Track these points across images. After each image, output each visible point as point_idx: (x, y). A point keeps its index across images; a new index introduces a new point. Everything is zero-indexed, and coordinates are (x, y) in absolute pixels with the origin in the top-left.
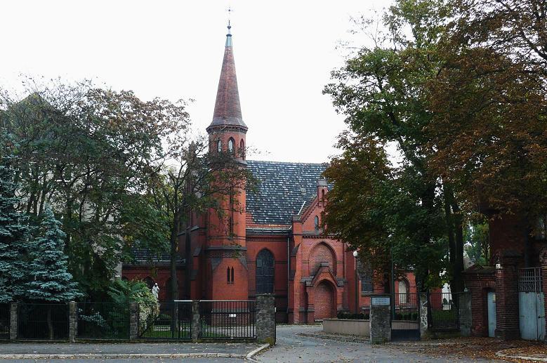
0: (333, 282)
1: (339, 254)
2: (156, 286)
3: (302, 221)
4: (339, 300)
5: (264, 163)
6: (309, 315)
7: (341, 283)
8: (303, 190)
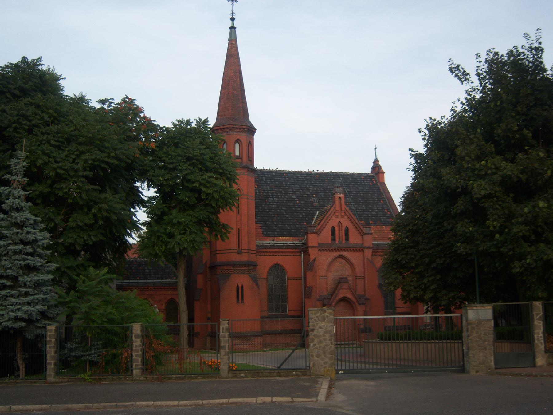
0: (354, 300)
1: (359, 269)
3: (318, 233)
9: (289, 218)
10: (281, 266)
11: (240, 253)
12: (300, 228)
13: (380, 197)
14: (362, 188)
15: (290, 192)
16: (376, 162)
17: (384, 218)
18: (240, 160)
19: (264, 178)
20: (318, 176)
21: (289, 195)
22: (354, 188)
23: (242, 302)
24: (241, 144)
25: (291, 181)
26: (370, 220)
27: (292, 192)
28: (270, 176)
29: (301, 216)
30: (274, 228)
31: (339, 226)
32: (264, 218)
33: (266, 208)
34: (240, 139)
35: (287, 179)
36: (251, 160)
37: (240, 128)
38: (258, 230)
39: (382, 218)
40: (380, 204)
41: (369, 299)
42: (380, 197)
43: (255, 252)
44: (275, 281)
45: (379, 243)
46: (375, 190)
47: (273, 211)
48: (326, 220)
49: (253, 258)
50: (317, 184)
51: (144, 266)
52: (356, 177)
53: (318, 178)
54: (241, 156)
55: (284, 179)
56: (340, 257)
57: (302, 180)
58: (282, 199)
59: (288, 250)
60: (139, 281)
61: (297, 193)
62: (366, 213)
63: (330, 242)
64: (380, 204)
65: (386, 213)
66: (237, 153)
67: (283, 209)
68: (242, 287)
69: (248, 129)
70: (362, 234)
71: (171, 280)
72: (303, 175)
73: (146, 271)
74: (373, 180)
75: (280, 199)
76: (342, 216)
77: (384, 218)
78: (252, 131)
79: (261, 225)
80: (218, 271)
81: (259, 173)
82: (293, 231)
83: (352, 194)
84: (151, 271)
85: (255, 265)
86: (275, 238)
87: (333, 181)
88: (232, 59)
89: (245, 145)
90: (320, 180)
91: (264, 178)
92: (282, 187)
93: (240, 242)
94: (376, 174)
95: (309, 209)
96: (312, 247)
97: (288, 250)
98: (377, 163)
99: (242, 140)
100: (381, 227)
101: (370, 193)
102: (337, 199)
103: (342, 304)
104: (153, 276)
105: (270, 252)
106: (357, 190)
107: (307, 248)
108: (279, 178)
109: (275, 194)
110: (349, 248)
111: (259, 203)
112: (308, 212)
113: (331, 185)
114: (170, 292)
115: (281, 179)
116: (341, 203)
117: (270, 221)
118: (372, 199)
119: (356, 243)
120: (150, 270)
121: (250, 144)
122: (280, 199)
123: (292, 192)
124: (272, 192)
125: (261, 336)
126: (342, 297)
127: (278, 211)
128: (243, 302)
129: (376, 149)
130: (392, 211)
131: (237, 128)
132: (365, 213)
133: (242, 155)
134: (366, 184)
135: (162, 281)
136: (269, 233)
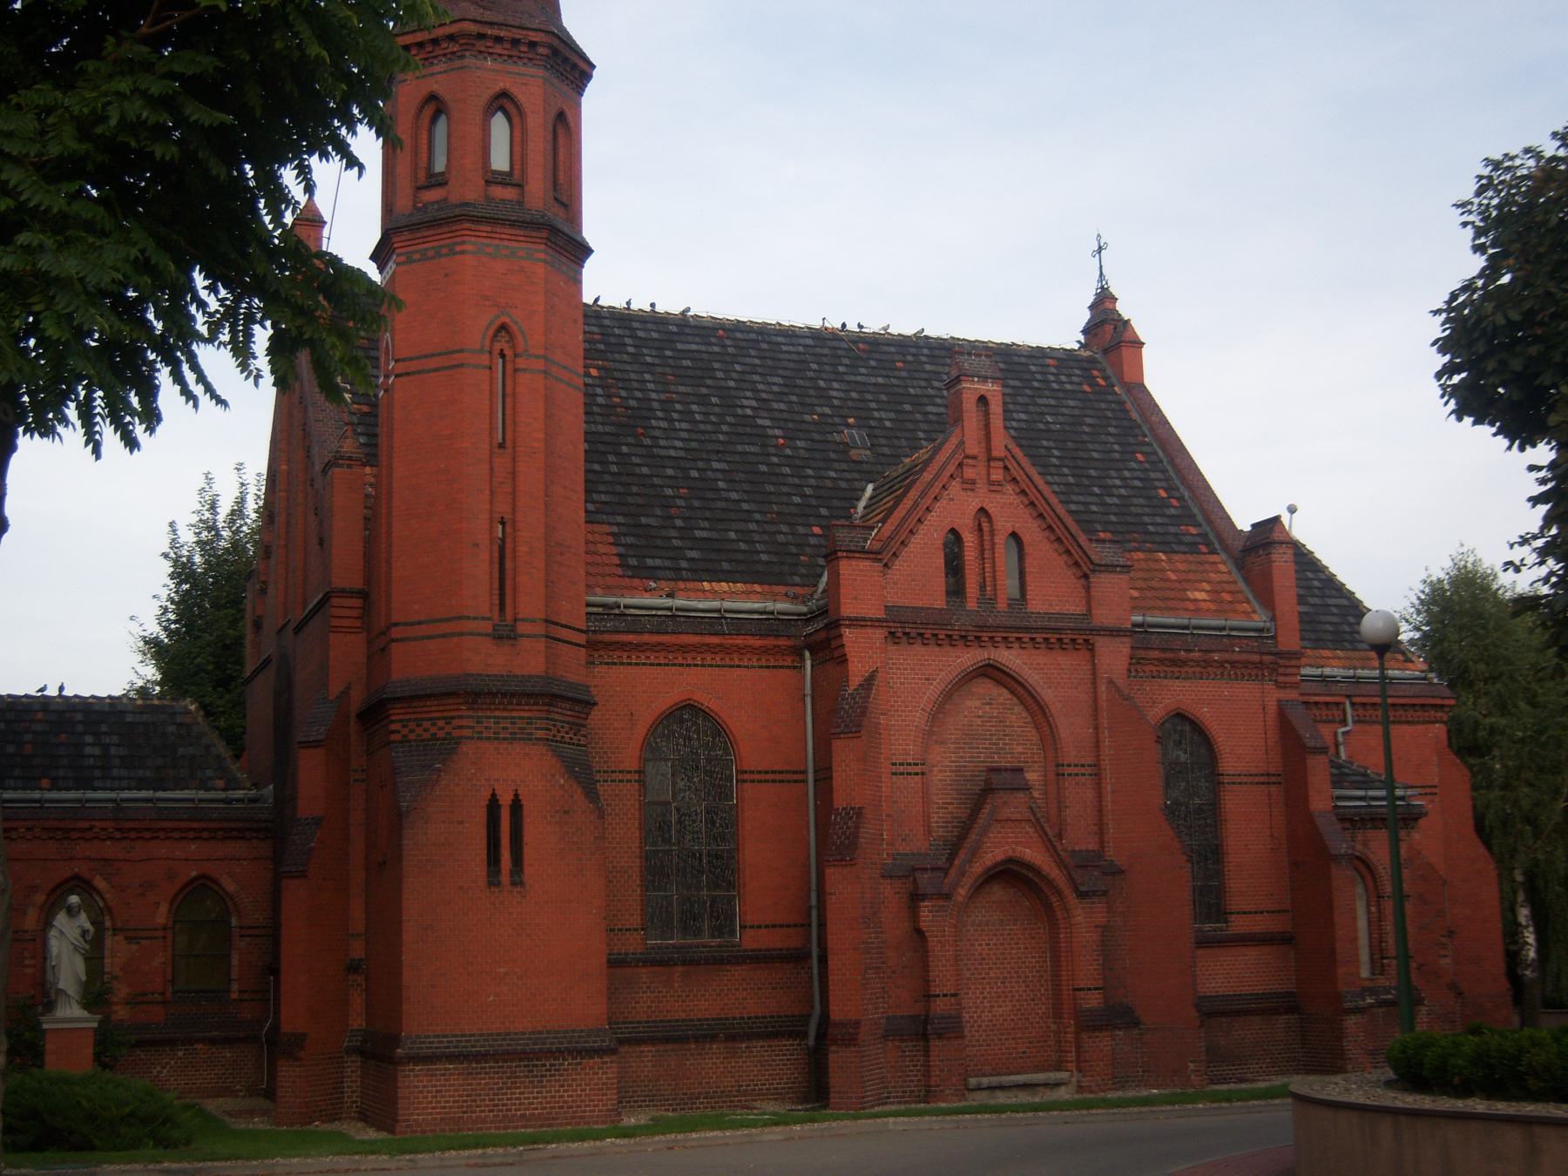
0: (1054, 873)
1: (1072, 730)
2: (71, 912)
3: (883, 556)
8: (852, 434)
9: (745, 506)
10: (707, 715)
11: (505, 634)
12: (793, 549)
13: (1132, 440)
14: (1052, 402)
15: (745, 402)
16: (1103, 303)
17: (1159, 520)
18: (510, 193)
19: (628, 341)
20: (861, 346)
21: (739, 411)
22: (1020, 399)
23: (514, 884)
24: (516, 120)
25: (748, 360)
26: (1099, 527)
27: (754, 403)
28: (655, 335)
29: (797, 500)
30: (676, 543)
31: (980, 529)
32: (630, 500)
33: (635, 460)
34: (515, 91)
35: (730, 350)
36: (564, 199)
37: (515, 42)
38: (601, 549)
39: (1146, 519)
40: (1133, 465)
41: (1122, 872)
42: (1132, 440)
43: (582, 639)
44: (681, 784)
45: (1149, 619)
46: (1109, 414)
47: (670, 472)
48: (923, 494)
49: (572, 667)
50: (859, 378)
51: (80, 728)
52: (1023, 360)
53: (864, 355)
54: (517, 173)
55: (716, 349)
56: (984, 675)
57: (795, 357)
58: (709, 427)
59: (739, 641)
61: (775, 405)
62: (1081, 498)
63: (939, 602)
64: (1133, 465)
65: (1164, 504)
66: (500, 160)
67: (715, 465)
68: (517, 805)
69: (555, 52)
70: (1085, 569)
71: (202, 794)
72: (802, 341)
73: (88, 750)
74: (1095, 373)
75: (702, 427)
76: (991, 483)
77: (1159, 520)
78: (575, 66)
79: (615, 529)
80: (393, 727)
81: (607, 322)
82: (764, 557)
84: (113, 750)
85: (586, 704)
86: (681, 585)
87: (928, 367)
89: (537, 122)
90: (873, 363)
91: (628, 341)
92: (709, 382)
93: (509, 583)
94: (1106, 351)
95: (833, 474)
96: (858, 622)
97: (739, 641)
98: (1108, 305)
99: (521, 98)
100: (1149, 555)
101: (1089, 420)
102: (969, 404)
103: (998, 892)
104: (115, 772)
105: (654, 648)
106: (1032, 409)
107: (835, 624)
108: (694, 347)
109: (678, 407)
110: (1027, 629)
111: (606, 438)
112: (828, 483)
113: (923, 383)
114: (193, 847)
115: (703, 348)
116: (987, 426)
117: (658, 512)
118: (1097, 446)
119: (1057, 609)
120: (106, 747)
121: (564, 128)
122: (702, 427)
123: (754, 403)
124: (663, 397)
125: (612, 1051)
126: (999, 858)
127: (694, 474)
128: (522, 883)
129: (1100, 249)
130: (1186, 495)
131: (498, 39)
132: (1075, 498)
133: (523, 171)
134: (1068, 387)
135: (161, 794)
136: (650, 562)
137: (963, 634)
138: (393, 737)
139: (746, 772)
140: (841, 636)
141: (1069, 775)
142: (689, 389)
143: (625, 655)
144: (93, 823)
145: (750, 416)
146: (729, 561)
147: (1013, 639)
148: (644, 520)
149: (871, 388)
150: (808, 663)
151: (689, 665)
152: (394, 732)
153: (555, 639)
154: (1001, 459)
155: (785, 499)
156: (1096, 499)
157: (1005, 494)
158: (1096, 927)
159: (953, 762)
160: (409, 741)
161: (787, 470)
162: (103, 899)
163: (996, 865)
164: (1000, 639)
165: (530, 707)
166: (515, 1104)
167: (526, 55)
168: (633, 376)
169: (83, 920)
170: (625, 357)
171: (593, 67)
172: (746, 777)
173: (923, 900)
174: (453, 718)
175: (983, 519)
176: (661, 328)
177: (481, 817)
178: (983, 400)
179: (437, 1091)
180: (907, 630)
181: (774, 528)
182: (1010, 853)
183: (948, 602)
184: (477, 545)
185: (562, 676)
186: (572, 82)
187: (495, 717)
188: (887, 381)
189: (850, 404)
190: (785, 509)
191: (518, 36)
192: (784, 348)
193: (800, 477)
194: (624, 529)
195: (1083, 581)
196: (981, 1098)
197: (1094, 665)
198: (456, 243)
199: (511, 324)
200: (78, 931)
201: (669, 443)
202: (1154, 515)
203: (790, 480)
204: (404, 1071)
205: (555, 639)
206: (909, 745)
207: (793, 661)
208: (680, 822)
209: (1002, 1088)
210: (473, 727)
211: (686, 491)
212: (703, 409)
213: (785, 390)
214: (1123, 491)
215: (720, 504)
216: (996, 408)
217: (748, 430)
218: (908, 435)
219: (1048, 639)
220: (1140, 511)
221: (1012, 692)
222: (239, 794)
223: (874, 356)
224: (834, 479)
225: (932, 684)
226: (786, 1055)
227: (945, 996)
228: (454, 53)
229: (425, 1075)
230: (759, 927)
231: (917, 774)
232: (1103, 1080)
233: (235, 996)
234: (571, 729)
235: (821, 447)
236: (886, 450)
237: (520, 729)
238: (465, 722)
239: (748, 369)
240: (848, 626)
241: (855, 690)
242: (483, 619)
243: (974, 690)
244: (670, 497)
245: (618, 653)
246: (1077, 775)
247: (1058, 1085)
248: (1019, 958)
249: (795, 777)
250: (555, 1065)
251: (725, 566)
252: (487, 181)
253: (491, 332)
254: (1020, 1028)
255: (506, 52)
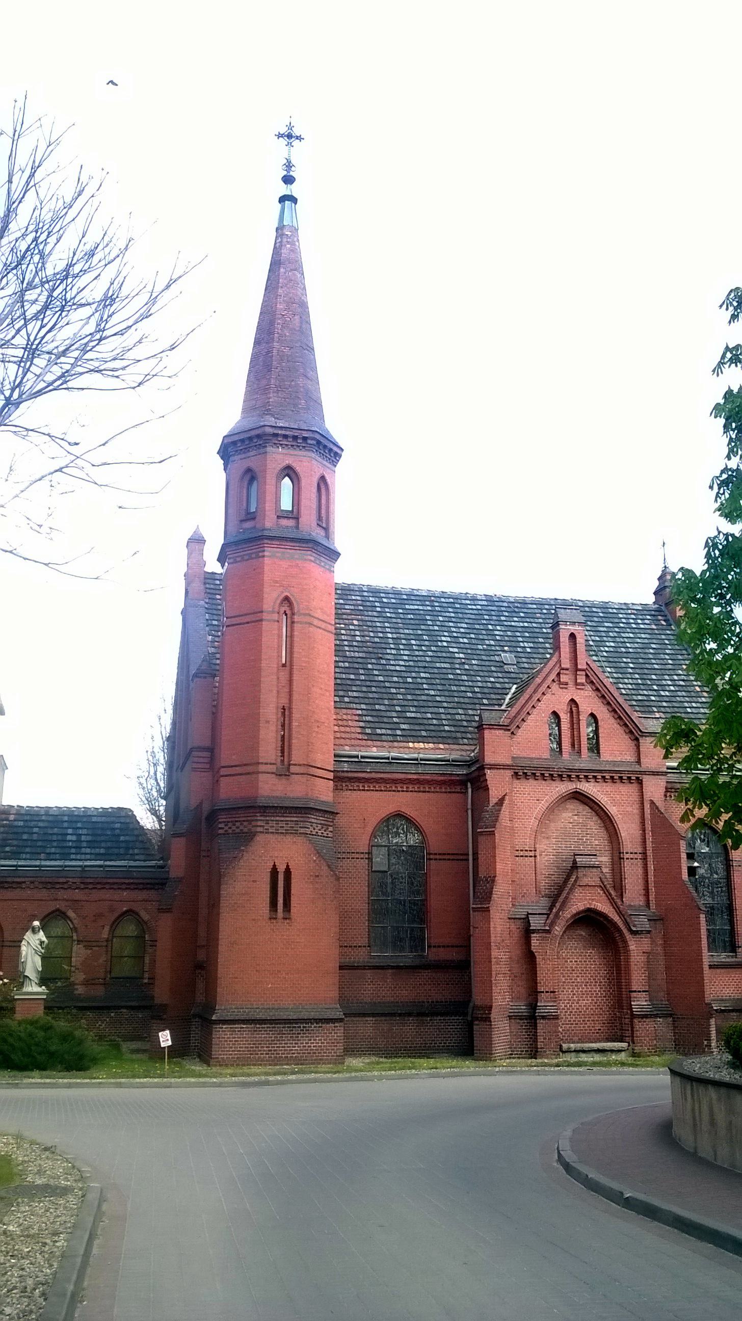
0: (616, 918)
1: (628, 830)
2: (34, 931)
3: (510, 728)
4: (638, 979)
5: (397, 593)
6: (541, 1024)
7: (642, 923)
8: (508, 657)
9: (438, 699)
11: (285, 772)
12: (465, 724)
14: (631, 635)
15: (443, 639)
18: (291, 523)
21: (440, 644)
22: (611, 634)
23: (285, 919)
25: (447, 614)
28: (393, 601)
29: (469, 695)
31: (571, 712)
32: (371, 695)
33: (376, 672)
34: (294, 465)
37: (295, 438)
43: (331, 776)
44: (393, 861)
46: (667, 642)
47: (395, 679)
50: (513, 624)
51: (66, 825)
55: (429, 608)
57: (475, 612)
58: (421, 653)
60: (43, 863)
61: (461, 640)
62: (645, 692)
67: (422, 675)
68: (288, 872)
69: (319, 442)
71: (132, 863)
72: (480, 603)
73: (69, 838)
75: (417, 653)
77: (694, 705)
81: (365, 594)
82: (447, 728)
83: (607, 649)
88: (282, 270)
90: (522, 615)
92: (423, 627)
94: (667, 605)
95: (492, 680)
96: (494, 767)
99: (298, 469)
107: (482, 768)
108: (416, 607)
109: (404, 642)
111: (359, 660)
112: (489, 685)
114: (125, 893)
115: (421, 608)
117: (386, 702)
118: (658, 661)
119: (619, 759)
122: (417, 653)
123: (449, 639)
124: (395, 636)
125: (341, 1020)
127: (409, 680)
128: (289, 919)
131: (285, 437)
134: (642, 626)
135: (108, 863)
136: (379, 731)
137: (560, 773)
138: (221, 831)
139: (432, 854)
140: (485, 774)
141: (627, 859)
142: (411, 632)
143: (361, 785)
144: (68, 879)
145: (445, 647)
146: (426, 731)
147: (591, 777)
148: (377, 707)
149: (520, 629)
150: (470, 790)
151: (399, 791)
152: (220, 828)
153: (313, 776)
154: (583, 670)
155: (462, 694)
156: (655, 693)
157: (586, 690)
158: (644, 952)
159: (555, 850)
160: (228, 834)
161: (465, 678)
162: (72, 923)
163: (578, 913)
164: (583, 777)
165: (297, 815)
166: (281, 1050)
167: (301, 445)
168: (378, 624)
169: (41, 935)
170: (375, 614)
171: (342, 450)
172: (432, 857)
173: (533, 933)
174: (253, 821)
175: (573, 706)
176: (397, 596)
177: (267, 878)
178: (573, 636)
179: (235, 1041)
180: (525, 771)
181: (454, 711)
182: (588, 906)
183: (551, 755)
184: (268, 722)
185: (317, 797)
186: (329, 459)
187: (276, 821)
188: (530, 625)
189: (506, 638)
190: (462, 700)
191: (296, 434)
192: (470, 607)
193: (472, 681)
194: (365, 712)
195: (636, 742)
196: (571, 1058)
197: (642, 792)
198: (260, 552)
199: (291, 597)
200: (38, 942)
201: (397, 662)
202: (691, 702)
203: (466, 683)
204: (216, 1028)
205: (313, 776)
206: (526, 839)
207: (461, 789)
208: (392, 883)
209: (584, 1051)
210: (263, 826)
211: (404, 690)
212: (418, 643)
213: (468, 631)
214: (672, 688)
215: (423, 698)
216: (580, 640)
217: (444, 655)
218: (540, 656)
219: (605, 776)
220: (682, 700)
221: (591, 808)
222: (153, 863)
223: (524, 610)
224: (493, 682)
225: (541, 803)
226: (454, 1026)
227: (547, 992)
228: (260, 445)
229: (229, 1031)
230: (439, 947)
231: (531, 856)
232: (648, 1049)
233: (146, 981)
234: (322, 828)
235: (487, 663)
236: (526, 665)
237: (291, 827)
238: (259, 823)
239: (447, 619)
240: (490, 769)
241: (493, 806)
242: (271, 764)
243: (567, 807)
244: (394, 693)
245: (357, 784)
246: (632, 859)
247: (619, 1051)
248: (595, 970)
249: (461, 857)
250: (306, 1027)
251: (424, 733)
252: (278, 516)
253: (278, 602)
254: (596, 1015)
255: (290, 443)
